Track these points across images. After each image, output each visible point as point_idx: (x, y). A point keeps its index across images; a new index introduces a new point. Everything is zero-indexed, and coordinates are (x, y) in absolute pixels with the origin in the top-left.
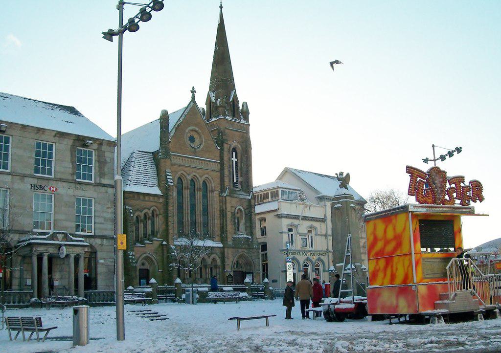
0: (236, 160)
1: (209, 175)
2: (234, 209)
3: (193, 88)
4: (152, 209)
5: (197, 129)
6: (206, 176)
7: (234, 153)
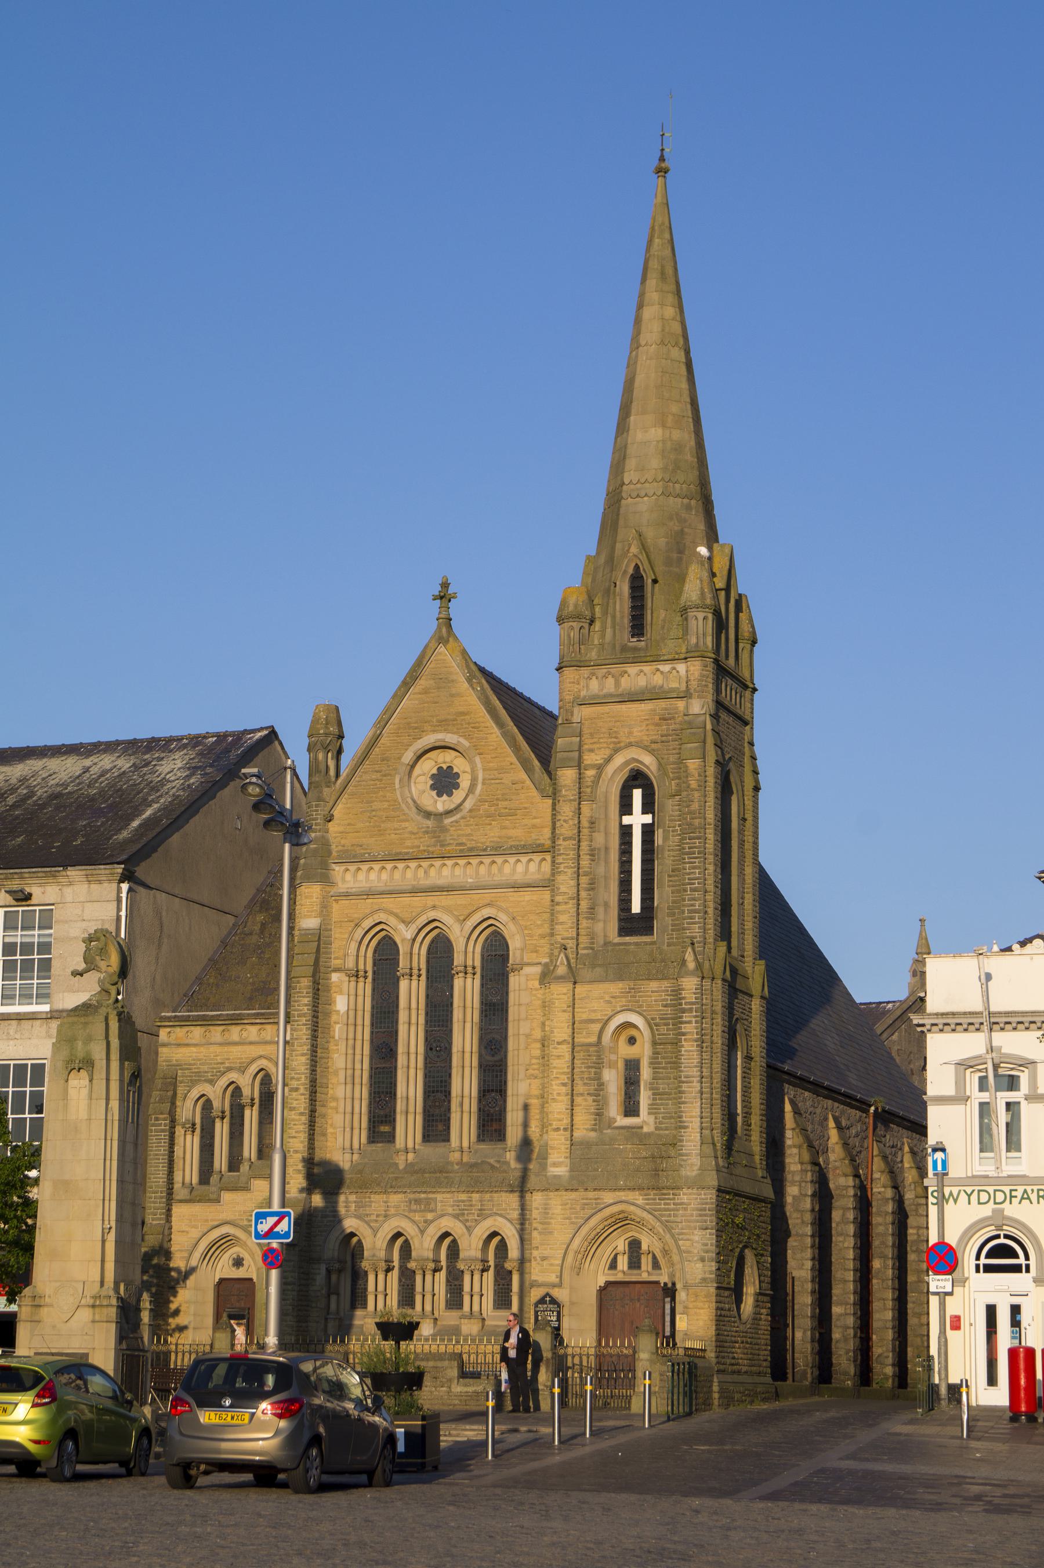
0: (648, 819)
1: (500, 909)
2: (597, 1027)
3: (445, 585)
4: (254, 1068)
5: (451, 739)
6: (486, 912)
7: (637, 794)
